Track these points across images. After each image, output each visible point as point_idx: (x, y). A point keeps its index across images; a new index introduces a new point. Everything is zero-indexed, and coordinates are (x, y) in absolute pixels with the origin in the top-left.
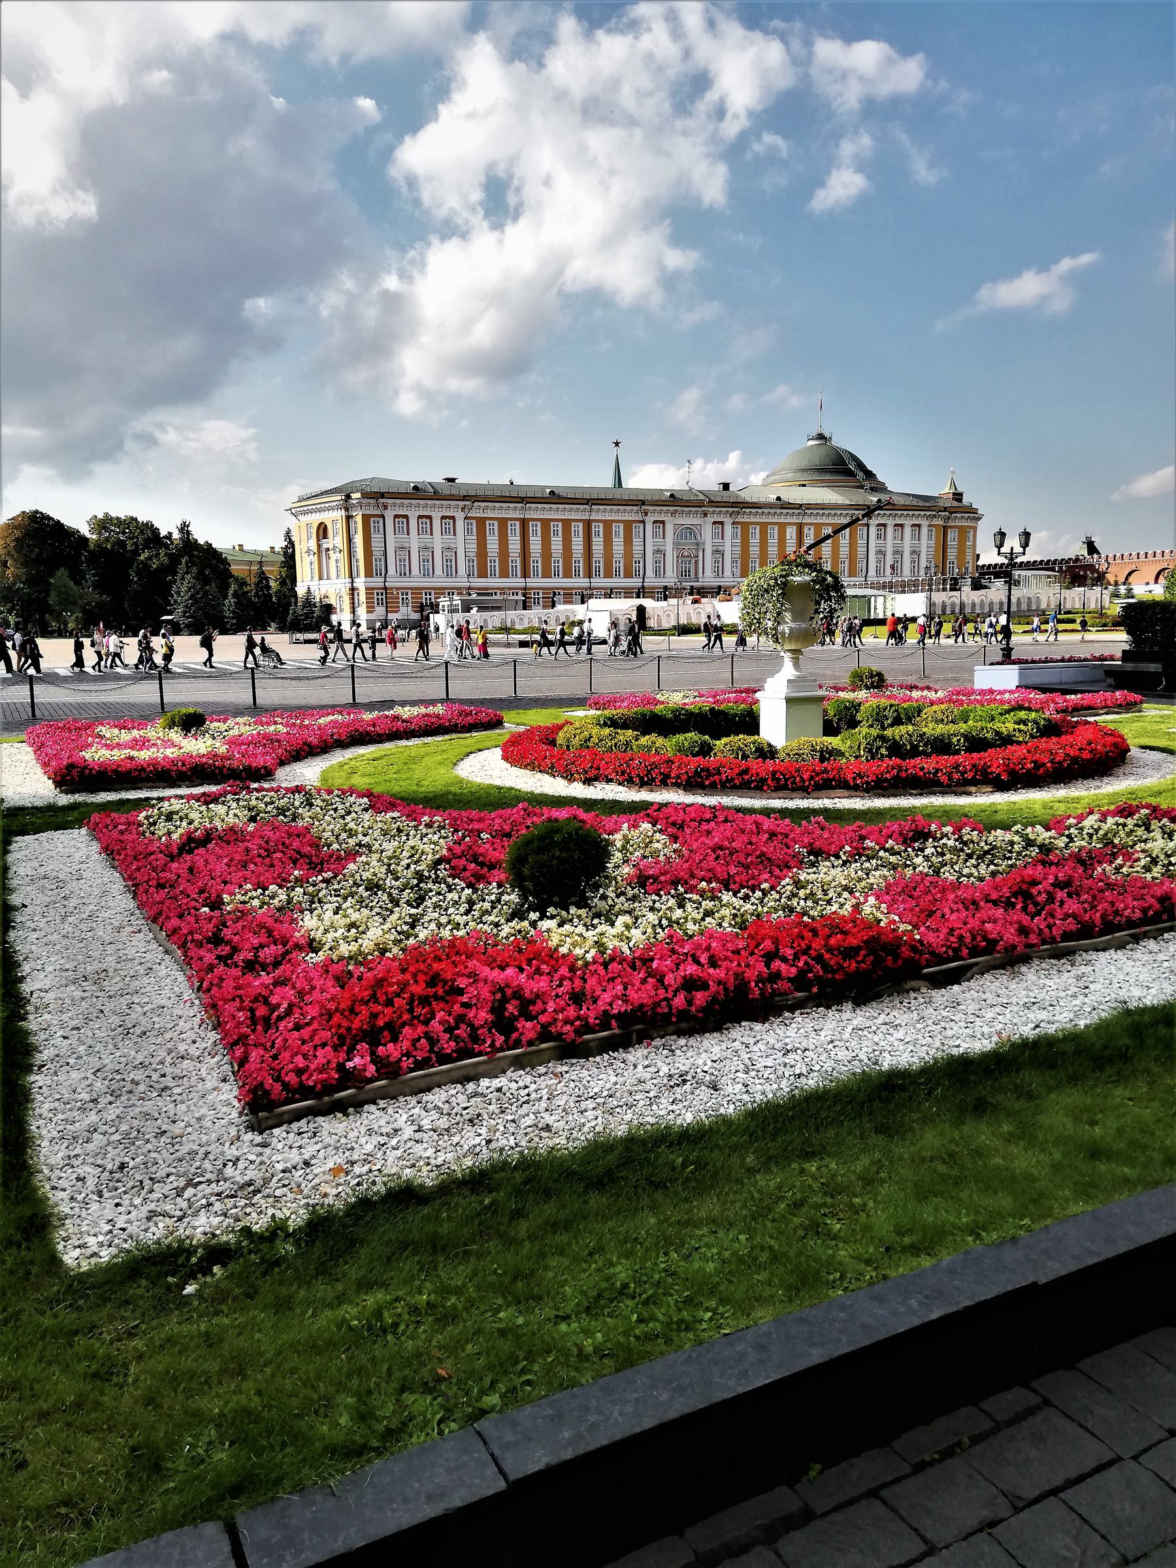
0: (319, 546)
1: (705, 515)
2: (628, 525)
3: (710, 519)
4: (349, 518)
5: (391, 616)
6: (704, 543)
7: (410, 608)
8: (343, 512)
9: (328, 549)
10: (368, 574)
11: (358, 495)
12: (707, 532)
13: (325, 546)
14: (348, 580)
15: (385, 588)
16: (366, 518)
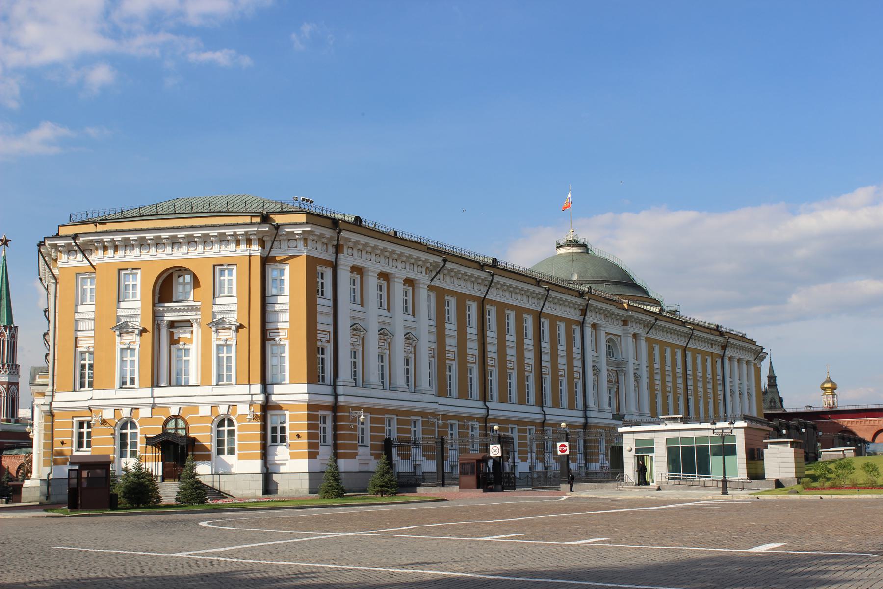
0: (156, 316)
1: (625, 323)
2: (569, 322)
3: (632, 329)
4: (266, 261)
5: (344, 465)
6: (626, 363)
7: (368, 450)
8: (256, 250)
9: (172, 324)
10: (313, 377)
11: (302, 218)
12: (627, 349)
13: (169, 317)
14: (257, 388)
15: (335, 408)
16: (312, 263)
